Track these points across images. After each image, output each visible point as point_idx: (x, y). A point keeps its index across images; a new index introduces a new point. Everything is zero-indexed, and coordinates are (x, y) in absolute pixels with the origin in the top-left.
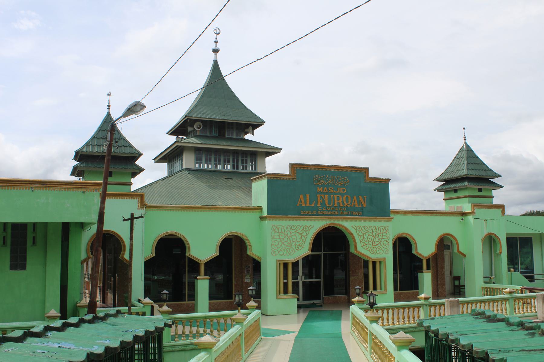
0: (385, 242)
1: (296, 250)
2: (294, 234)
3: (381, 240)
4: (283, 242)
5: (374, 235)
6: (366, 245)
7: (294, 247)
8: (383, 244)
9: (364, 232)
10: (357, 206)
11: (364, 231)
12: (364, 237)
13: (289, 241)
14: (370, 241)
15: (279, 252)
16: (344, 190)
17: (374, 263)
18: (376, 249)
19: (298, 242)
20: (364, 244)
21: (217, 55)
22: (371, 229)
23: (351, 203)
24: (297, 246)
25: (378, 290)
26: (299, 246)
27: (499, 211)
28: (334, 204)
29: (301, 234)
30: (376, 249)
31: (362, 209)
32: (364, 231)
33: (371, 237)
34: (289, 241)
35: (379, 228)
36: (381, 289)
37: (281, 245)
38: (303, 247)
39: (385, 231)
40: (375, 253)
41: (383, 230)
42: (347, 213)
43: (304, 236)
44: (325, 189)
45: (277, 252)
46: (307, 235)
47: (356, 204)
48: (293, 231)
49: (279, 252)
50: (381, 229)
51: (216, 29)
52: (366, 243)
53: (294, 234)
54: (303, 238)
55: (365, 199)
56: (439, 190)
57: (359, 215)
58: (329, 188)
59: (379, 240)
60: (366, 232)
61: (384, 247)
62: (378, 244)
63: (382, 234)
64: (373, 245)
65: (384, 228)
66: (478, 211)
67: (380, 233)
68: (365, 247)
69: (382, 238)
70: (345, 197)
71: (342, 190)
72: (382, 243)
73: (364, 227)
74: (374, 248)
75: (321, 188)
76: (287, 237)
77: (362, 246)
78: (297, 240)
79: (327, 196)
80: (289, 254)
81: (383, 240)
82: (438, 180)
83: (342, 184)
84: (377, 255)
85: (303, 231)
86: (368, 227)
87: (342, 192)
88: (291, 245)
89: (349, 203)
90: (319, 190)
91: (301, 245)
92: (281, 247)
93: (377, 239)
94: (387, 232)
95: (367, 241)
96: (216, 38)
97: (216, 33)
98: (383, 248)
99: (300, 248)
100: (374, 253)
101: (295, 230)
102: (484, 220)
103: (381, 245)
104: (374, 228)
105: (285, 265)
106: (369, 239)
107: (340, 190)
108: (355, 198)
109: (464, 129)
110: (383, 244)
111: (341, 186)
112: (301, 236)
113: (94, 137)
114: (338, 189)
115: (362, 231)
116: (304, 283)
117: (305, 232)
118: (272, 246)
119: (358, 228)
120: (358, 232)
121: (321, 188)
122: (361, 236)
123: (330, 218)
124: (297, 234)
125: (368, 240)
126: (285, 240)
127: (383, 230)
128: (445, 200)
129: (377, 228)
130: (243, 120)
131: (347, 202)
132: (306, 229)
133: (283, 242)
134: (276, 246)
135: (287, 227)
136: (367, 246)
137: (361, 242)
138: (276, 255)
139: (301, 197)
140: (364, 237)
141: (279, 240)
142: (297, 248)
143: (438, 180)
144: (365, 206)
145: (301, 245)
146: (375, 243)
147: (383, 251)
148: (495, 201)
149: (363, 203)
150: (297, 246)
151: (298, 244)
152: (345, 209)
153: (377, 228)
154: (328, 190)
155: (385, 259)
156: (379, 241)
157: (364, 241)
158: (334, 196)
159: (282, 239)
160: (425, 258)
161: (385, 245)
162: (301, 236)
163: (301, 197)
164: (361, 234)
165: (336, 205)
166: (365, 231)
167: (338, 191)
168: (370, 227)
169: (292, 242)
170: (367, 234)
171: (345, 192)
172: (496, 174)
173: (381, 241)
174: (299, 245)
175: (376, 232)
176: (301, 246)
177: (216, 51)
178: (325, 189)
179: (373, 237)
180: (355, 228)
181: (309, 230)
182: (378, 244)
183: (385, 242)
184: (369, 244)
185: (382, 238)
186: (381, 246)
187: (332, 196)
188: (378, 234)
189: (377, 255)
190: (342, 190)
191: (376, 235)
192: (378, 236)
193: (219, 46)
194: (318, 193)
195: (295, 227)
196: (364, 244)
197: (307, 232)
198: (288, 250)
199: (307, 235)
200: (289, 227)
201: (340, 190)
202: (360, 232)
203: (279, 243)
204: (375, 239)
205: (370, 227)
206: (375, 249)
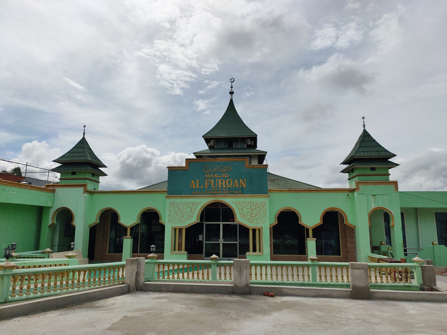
0: (262, 214)
1: (186, 219)
2: (186, 208)
3: (259, 212)
4: (177, 213)
5: (253, 208)
6: (245, 216)
7: (185, 217)
8: (261, 215)
9: (243, 206)
10: (237, 186)
11: (243, 206)
12: (243, 210)
13: (181, 212)
14: (249, 213)
15: (174, 221)
16: (227, 175)
17: (254, 231)
18: (254, 220)
19: (188, 213)
20: (243, 216)
21: (232, 96)
22: (249, 204)
23: (233, 185)
24: (187, 217)
25: (250, 252)
26: (189, 217)
27: (392, 187)
28: (218, 186)
29: (191, 208)
30: (254, 220)
31: (242, 189)
32: (243, 206)
33: (249, 210)
34: (181, 212)
35: (257, 203)
36: (260, 251)
37: (176, 216)
38: (192, 217)
39: (262, 205)
40: (253, 222)
41: (261, 204)
42: (229, 192)
43: (194, 210)
44: (212, 175)
45: (173, 221)
46: (195, 209)
47: (237, 185)
48: (185, 206)
49: (174, 221)
50: (258, 204)
51: (231, 79)
52: (245, 215)
53: (186, 208)
54: (192, 211)
55: (245, 181)
56: (343, 171)
57: (239, 194)
58: (215, 175)
59: (257, 212)
60: (245, 206)
61: (261, 218)
62: (256, 216)
63: (259, 208)
64: (251, 216)
65: (261, 203)
66: (361, 187)
67: (258, 207)
68: (244, 218)
69: (260, 211)
70: (227, 181)
71: (225, 175)
72: (259, 215)
73: (243, 203)
74: (252, 219)
75: (209, 175)
76: (180, 210)
77: (241, 217)
78: (188, 213)
79: (212, 181)
80: (181, 223)
81: (260, 212)
82: (344, 163)
83: (225, 171)
84: (255, 224)
85: (193, 206)
86: (247, 203)
87: (225, 177)
88: (183, 216)
89: (231, 185)
90: (206, 176)
91: (190, 216)
92: (176, 217)
93: (255, 212)
94: (264, 207)
95: (245, 213)
96: (232, 85)
97: (231, 81)
98: (260, 219)
99: (190, 218)
100: (252, 222)
101: (186, 206)
102: (372, 196)
103: (258, 216)
104: (253, 203)
105: (175, 229)
106: (247, 212)
107: (224, 175)
108: (236, 181)
109: (363, 118)
110: (261, 215)
111: (225, 173)
112: (191, 210)
113: (68, 152)
114: (222, 175)
115: (241, 205)
116: (224, 244)
117: (194, 206)
118: (169, 216)
119: (239, 203)
120: (238, 206)
121: (209, 175)
122: (240, 209)
123: (215, 196)
124: (188, 208)
125: (247, 212)
126: (179, 212)
127: (261, 204)
128: (348, 179)
129: (255, 203)
130: (249, 135)
131: (229, 184)
132: (195, 204)
133: (177, 213)
134: (172, 216)
135: (181, 203)
136: (245, 217)
137: (240, 214)
138: (171, 223)
139: (193, 182)
140: (243, 210)
141: (174, 212)
142: (188, 218)
143: (344, 163)
144: (244, 186)
145: (190, 216)
146: (253, 214)
147: (261, 221)
148: (391, 178)
149: (243, 184)
150: (187, 217)
151: (188, 215)
152: (227, 189)
153: (255, 203)
154: (214, 176)
155: (262, 228)
156: (257, 213)
157: (243, 213)
158: (219, 180)
159: (176, 212)
160: (311, 228)
161: (263, 217)
162: (191, 210)
163: (193, 182)
164: (240, 208)
165: (220, 187)
166: (244, 205)
167: (222, 176)
168: (248, 203)
169: (184, 214)
170: (246, 208)
171: (228, 176)
172: (391, 153)
173: (258, 213)
174: (189, 216)
175: (254, 206)
176: (191, 217)
177: (232, 93)
178: (212, 175)
179: (251, 211)
180: (236, 203)
181: (198, 205)
182: (256, 216)
183: (262, 214)
184: (248, 215)
185: (260, 211)
186: (258, 218)
187: (217, 180)
188: (256, 207)
189: (255, 224)
190: (225, 175)
191: (254, 209)
192: (256, 209)
193: (234, 90)
194: (206, 179)
195: (187, 203)
196: (243, 216)
197: (196, 207)
198: (181, 219)
199: (195, 209)
200: (182, 203)
201: (224, 175)
202: (240, 206)
203: (174, 214)
204: (253, 212)
205: (248, 203)
206: (253, 220)
